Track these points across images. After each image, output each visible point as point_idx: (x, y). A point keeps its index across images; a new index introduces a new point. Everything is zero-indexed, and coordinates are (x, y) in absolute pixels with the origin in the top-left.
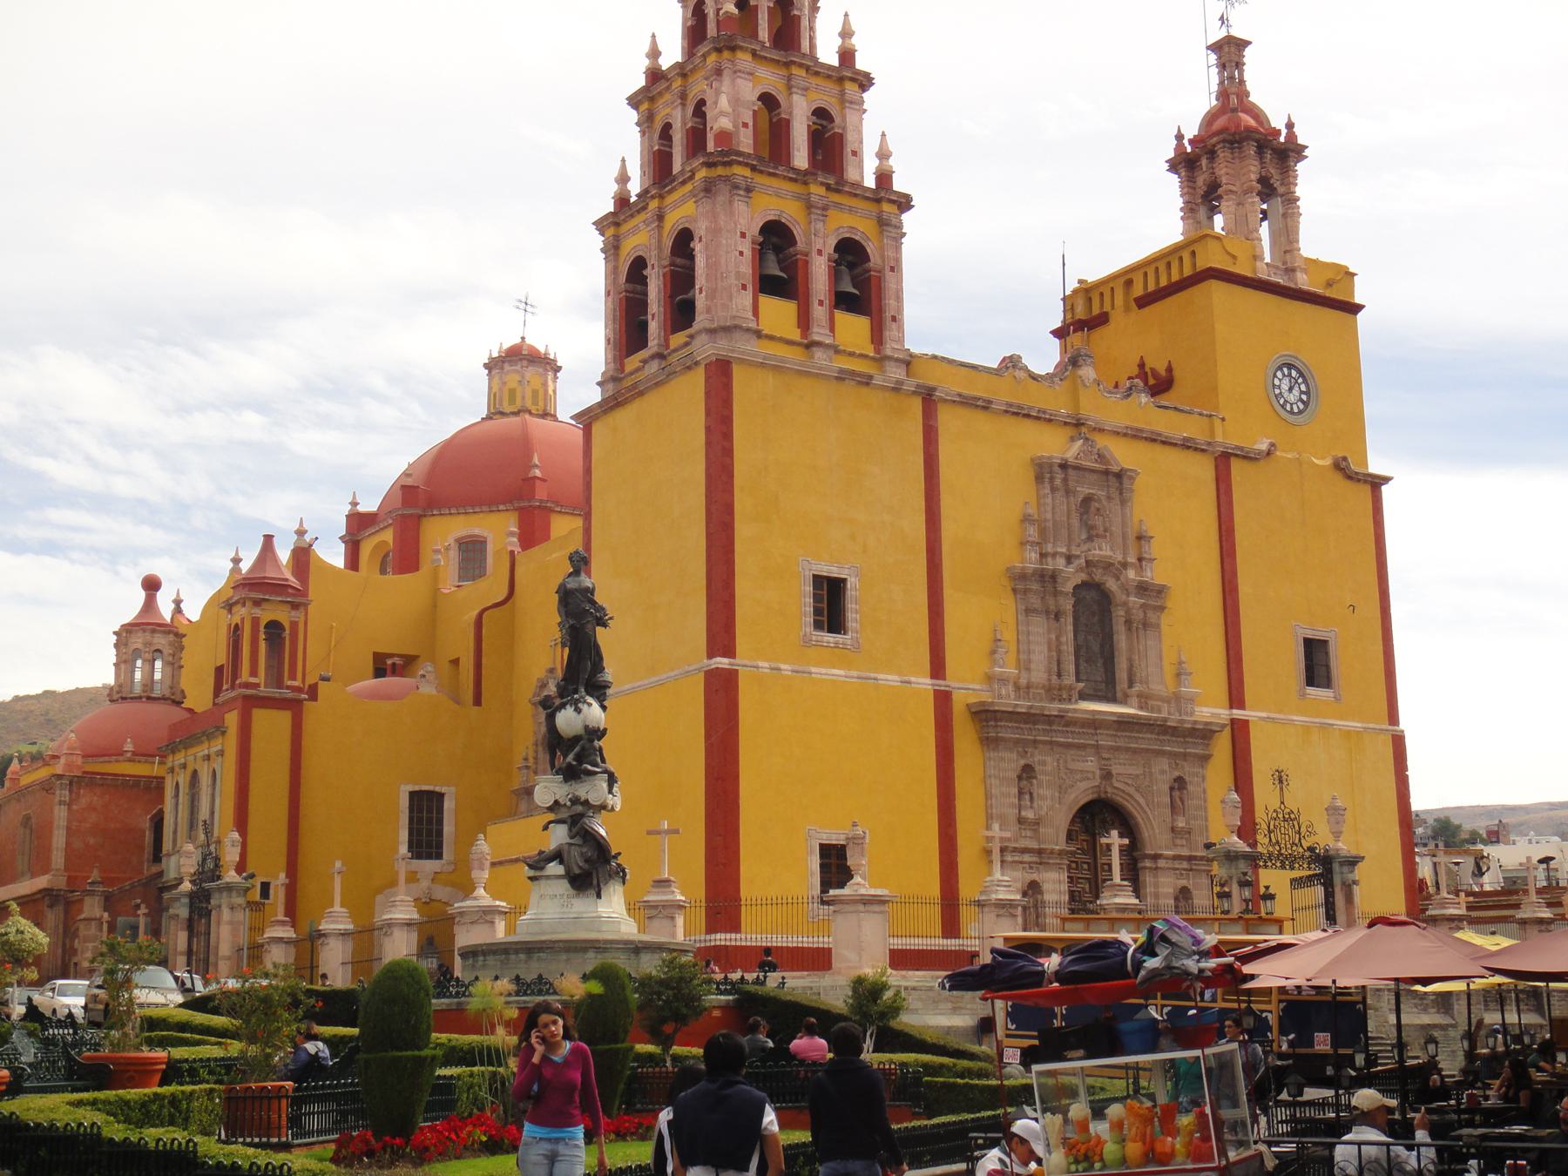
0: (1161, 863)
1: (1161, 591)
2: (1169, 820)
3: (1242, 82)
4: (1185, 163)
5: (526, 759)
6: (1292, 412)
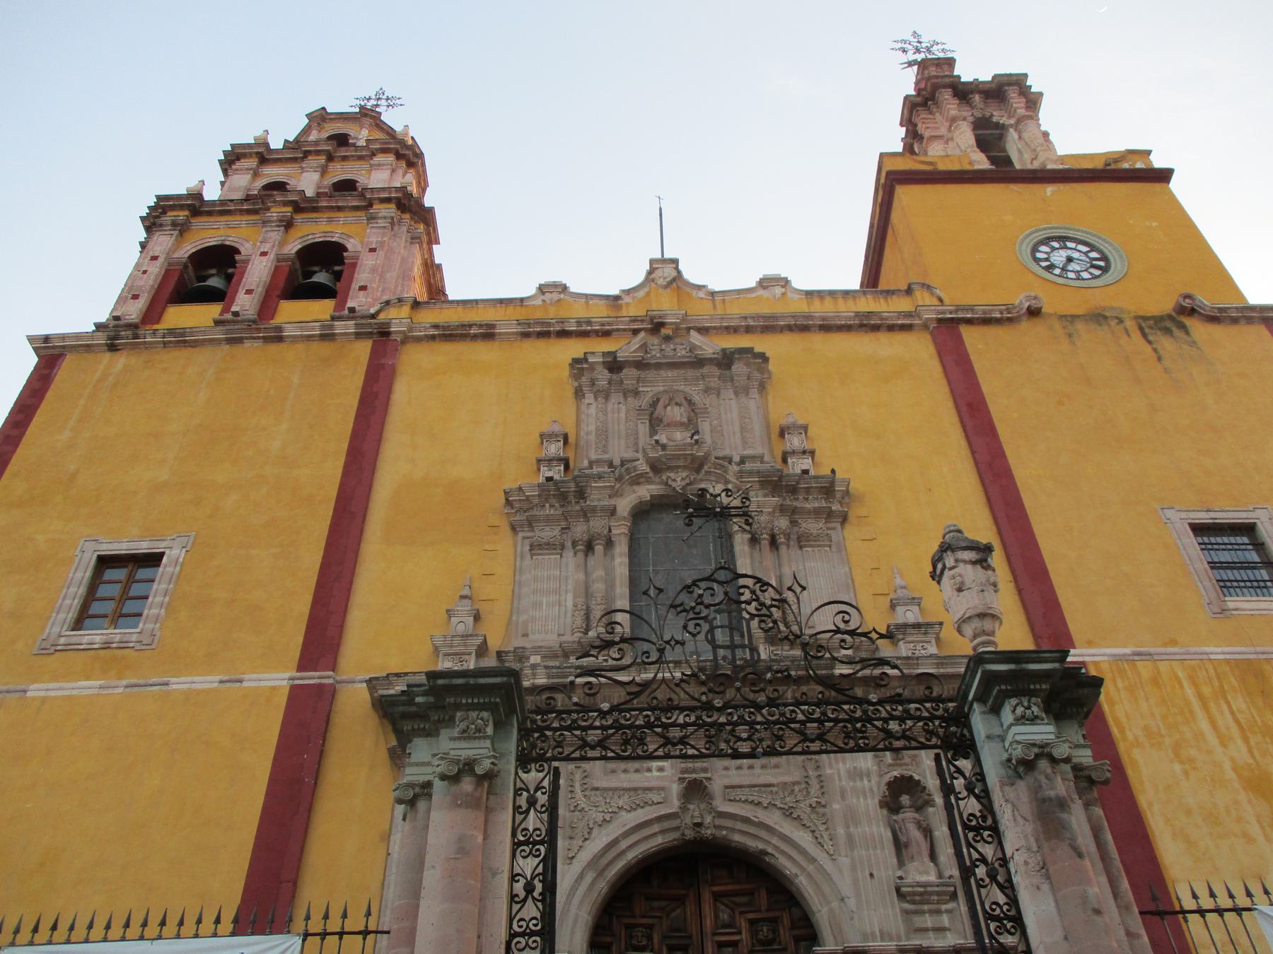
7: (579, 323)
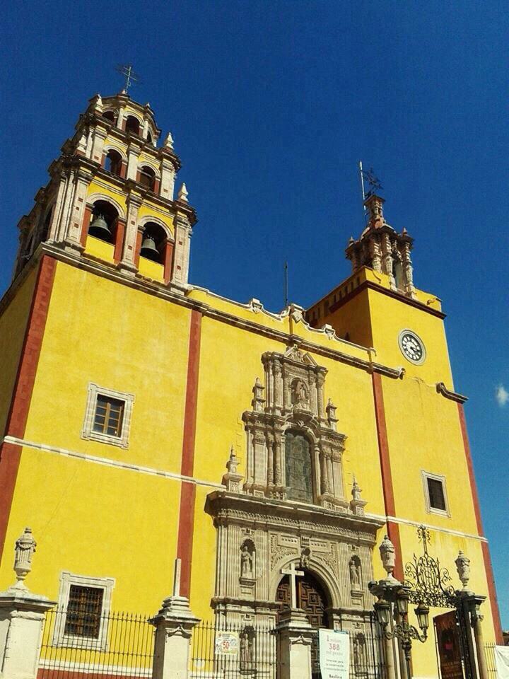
0: (344, 616)
1: (342, 438)
2: (349, 585)
6: (413, 359)
7: (267, 330)
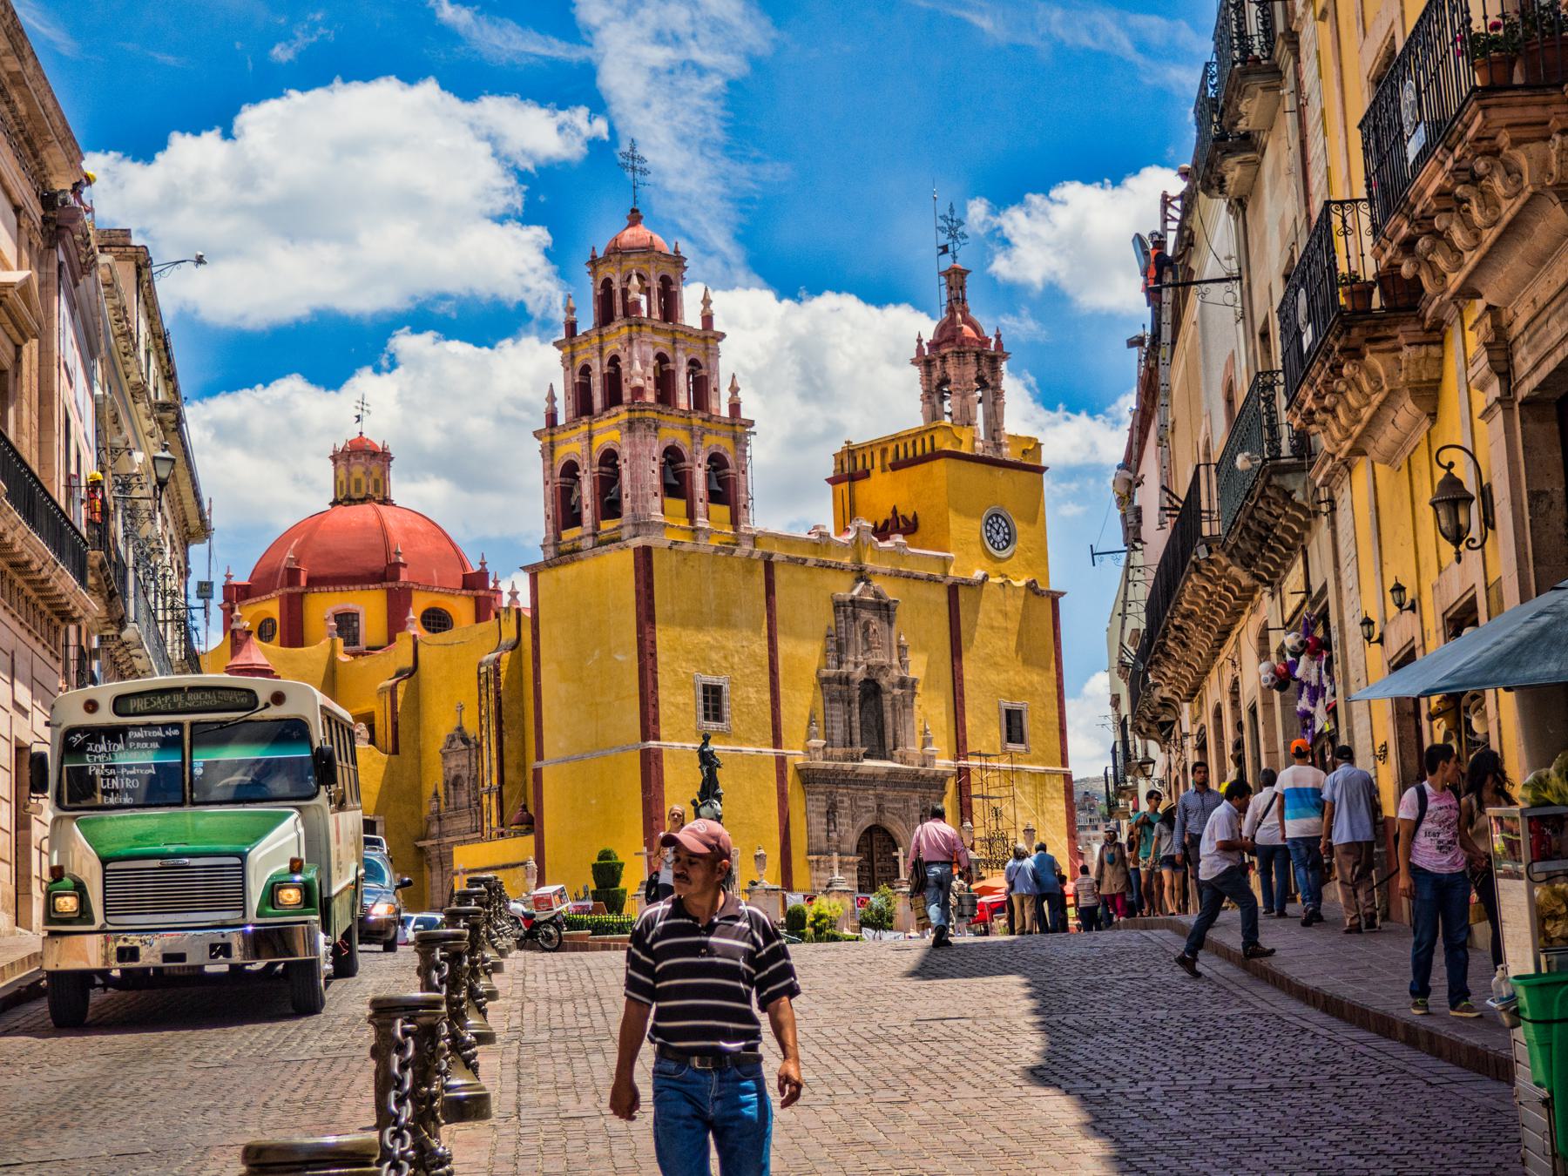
3: (964, 300)
4: (925, 362)
5: (436, 794)
6: (998, 549)
